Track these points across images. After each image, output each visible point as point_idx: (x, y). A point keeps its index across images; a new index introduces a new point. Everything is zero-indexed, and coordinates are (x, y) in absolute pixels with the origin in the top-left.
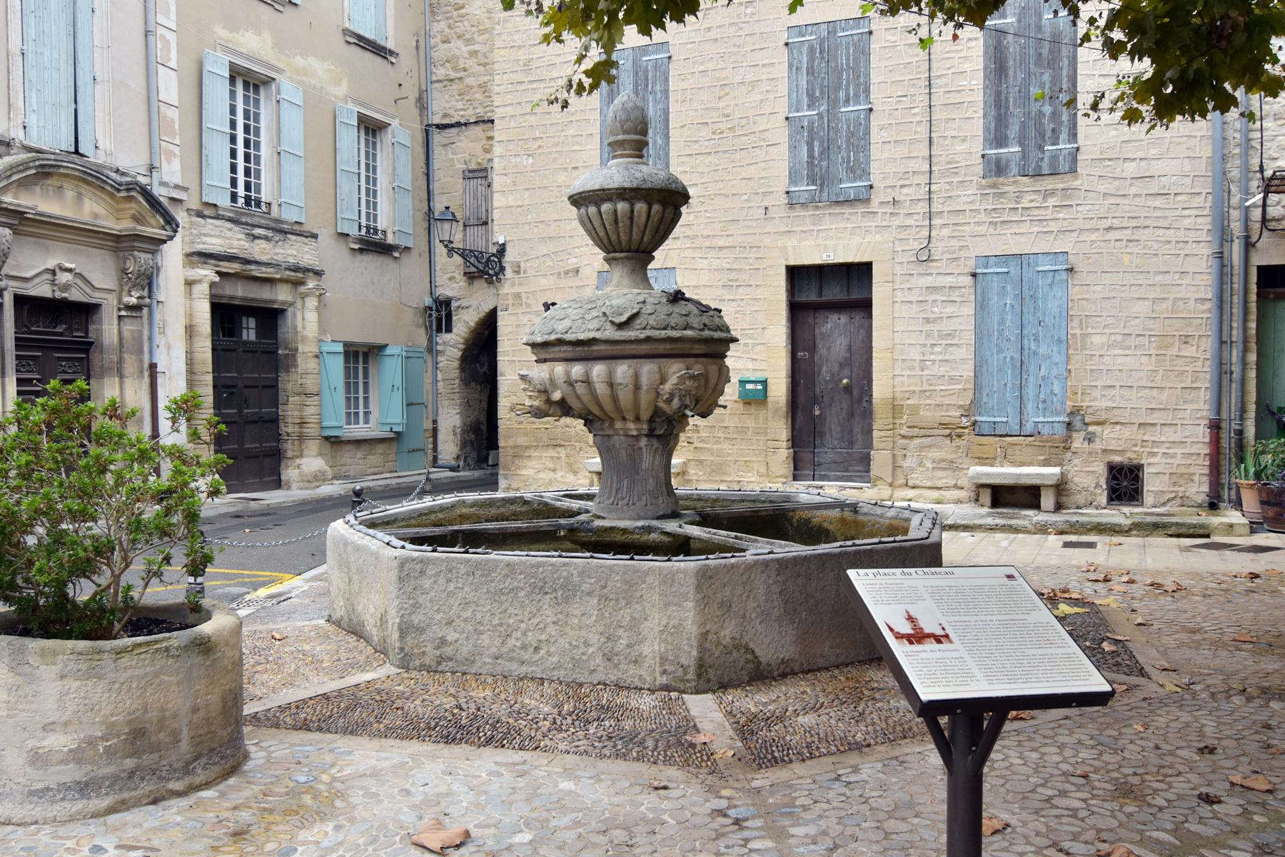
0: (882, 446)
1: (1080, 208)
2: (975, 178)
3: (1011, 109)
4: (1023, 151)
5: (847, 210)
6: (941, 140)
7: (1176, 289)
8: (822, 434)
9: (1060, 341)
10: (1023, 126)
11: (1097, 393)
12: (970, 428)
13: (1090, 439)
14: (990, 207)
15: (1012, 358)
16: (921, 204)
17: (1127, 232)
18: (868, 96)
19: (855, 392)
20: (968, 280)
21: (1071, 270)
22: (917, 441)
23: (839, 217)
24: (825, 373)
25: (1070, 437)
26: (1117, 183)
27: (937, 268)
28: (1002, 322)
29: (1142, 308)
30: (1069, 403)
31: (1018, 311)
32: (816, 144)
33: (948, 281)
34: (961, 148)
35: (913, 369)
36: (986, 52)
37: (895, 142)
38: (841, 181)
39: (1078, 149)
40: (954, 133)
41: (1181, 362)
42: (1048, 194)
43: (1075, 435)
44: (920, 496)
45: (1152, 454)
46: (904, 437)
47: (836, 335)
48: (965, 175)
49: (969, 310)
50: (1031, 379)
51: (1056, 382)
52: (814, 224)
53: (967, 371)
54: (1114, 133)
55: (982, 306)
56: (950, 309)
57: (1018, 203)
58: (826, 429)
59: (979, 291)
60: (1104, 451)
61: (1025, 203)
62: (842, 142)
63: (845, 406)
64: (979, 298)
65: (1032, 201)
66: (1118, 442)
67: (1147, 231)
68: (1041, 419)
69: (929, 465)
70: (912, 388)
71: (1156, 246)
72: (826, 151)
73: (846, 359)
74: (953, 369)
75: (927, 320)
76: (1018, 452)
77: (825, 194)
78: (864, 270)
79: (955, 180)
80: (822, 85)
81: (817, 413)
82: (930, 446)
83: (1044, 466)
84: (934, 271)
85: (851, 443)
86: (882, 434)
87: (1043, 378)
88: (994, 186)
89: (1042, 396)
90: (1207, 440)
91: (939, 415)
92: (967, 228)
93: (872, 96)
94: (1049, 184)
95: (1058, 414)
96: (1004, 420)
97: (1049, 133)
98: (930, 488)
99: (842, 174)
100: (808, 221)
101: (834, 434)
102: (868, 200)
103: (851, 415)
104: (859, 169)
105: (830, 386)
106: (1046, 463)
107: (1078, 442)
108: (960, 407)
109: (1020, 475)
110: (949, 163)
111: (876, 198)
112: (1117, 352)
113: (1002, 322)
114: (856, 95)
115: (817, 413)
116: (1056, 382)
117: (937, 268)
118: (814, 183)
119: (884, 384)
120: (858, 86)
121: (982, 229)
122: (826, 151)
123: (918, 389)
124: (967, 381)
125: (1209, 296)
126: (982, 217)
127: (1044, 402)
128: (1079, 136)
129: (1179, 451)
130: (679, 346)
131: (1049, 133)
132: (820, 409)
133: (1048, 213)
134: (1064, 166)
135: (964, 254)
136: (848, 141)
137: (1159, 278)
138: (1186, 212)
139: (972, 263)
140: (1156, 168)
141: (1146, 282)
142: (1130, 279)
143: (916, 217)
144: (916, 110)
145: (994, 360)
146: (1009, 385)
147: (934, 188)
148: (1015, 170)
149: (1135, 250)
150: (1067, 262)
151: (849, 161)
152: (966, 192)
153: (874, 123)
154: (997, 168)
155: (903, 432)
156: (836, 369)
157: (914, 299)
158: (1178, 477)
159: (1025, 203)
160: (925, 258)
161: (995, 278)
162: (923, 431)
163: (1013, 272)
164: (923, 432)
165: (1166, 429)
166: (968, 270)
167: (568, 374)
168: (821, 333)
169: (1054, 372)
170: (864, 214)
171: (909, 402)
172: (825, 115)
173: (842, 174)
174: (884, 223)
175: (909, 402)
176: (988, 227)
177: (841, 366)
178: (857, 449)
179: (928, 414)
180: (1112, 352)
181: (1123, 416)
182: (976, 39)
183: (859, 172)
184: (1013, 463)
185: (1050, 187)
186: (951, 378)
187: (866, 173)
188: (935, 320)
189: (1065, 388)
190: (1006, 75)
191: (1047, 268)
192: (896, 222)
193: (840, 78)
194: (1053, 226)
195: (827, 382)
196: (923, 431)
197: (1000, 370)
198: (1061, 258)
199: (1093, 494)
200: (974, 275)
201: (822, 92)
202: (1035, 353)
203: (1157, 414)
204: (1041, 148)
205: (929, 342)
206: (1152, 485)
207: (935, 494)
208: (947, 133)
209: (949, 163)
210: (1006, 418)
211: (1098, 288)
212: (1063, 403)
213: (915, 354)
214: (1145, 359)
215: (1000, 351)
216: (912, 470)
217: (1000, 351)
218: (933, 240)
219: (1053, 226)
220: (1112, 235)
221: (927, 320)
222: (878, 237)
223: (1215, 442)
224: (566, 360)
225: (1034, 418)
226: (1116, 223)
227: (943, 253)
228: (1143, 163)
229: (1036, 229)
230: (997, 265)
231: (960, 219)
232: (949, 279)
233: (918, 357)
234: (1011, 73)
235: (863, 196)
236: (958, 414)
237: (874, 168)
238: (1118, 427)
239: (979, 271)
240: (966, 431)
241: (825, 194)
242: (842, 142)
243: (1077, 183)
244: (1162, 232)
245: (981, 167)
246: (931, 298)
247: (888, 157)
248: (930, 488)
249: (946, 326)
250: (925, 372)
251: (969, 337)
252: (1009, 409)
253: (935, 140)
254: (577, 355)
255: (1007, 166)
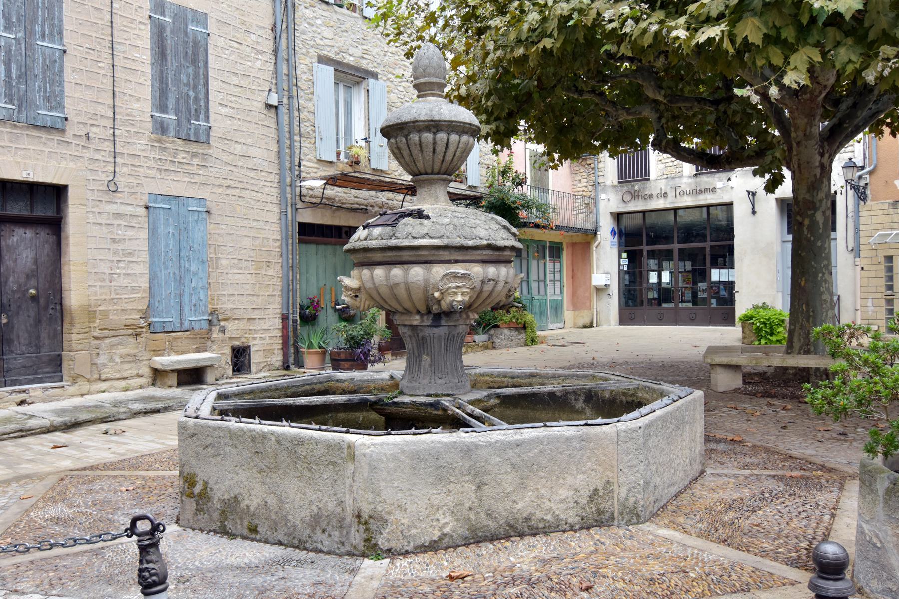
0: (80, 347)
1: (212, 170)
2: (147, 132)
3: (170, 86)
4: (178, 120)
5: (44, 135)
6: (121, 95)
7: (263, 231)
8: (10, 342)
9: (203, 262)
10: (178, 101)
11: (225, 299)
12: (148, 328)
13: (223, 330)
14: (158, 157)
15: (174, 273)
16: (107, 143)
17: (238, 190)
18: (62, 39)
19: (42, 301)
20: (143, 211)
21: (208, 212)
22: (108, 341)
23: (37, 140)
24: (12, 284)
25: (211, 330)
26: (232, 156)
27: (120, 198)
28: (167, 245)
29: (247, 242)
30: (210, 307)
31: (177, 238)
32: (14, 67)
33: (129, 209)
34: (136, 106)
35: (104, 280)
36: (152, 38)
37: (86, 86)
38: (38, 107)
39: (210, 128)
40: (130, 92)
41: (266, 278)
42: (195, 155)
43: (214, 329)
44: (111, 387)
45: (254, 339)
46: (96, 338)
47: (22, 247)
48: (140, 128)
49: (144, 235)
50: (187, 289)
51: (201, 292)
52: (11, 141)
53: (144, 283)
54: (229, 122)
55: (153, 232)
56: (130, 233)
57: (175, 157)
58: (14, 337)
59: (151, 221)
60: (230, 338)
61: (179, 159)
62: (38, 71)
63: (32, 314)
64: (151, 226)
65: (184, 158)
66: (236, 331)
67: (247, 192)
68: (194, 319)
69: (118, 360)
70: (103, 297)
71: (253, 202)
72: (24, 76)
73: (33, 271)
74: (134, 281)
75: (114, 240)
76: (180, 344)
77: (24, 116)
78: (58, 192)
79: (133, 130)
80: (18, 14)
81: (5, 321)
82: (118, 345)
83: (196, 352)
84: (119, 201)
85: (39, 348)
86: (80, 336)
87: (194, 289)
88: (160, 141)
89: (193, 302)
90: (280, 327)
91: (125, 319)
92: (141, 170)
93: (65, 40)
94: (194, 148)
95: (203, 314)
96: (171, 320)
97: (193, 112)
98: (118, 379)
99: (39, 101)
100: (6, 137)
101: (22, 341)
102: (63, 131)
103: (38, 322)
104: (55, 100)
105: (17, 296)
106: (198, 351)
107: (216, 334)
108: (140, 311)
109: (199, 360)
110: (128, 115)
111: (72, 130)
112: (236, 271)
113: (167, 245)
114: (52, 35)
115: (5, 321)
116: (201, 292)
117: (120, 198)
118: (11, 102)
119: (77, 292)
120: (52, 26)
121: (152, 173)
122: (24, 76)
123: (108, 297)
124: (144, 291)
125: (279, 238)
126: (152, 163)
127: (195, 306)
128: (211, 118)
129: (267, 335)
130: (389, 254)
131: (193, 112)
132: (8, 317)
133: (194, 169)
134: (203, 138)
135: (139, 190)
136: (44, 73)
137: (255, 223)
138: (266, 183)
139: (145, 198)
140: (253, 152)
141: (249, 225)
142: (240, 223)
143: (103, 153)
144: (101, 65)
145: (163, 275)
146: (173, 294)
147: (117, 132)
148: (172, 133)
149: (242, 203)
150: (205, 206)
151: (45, 91)
152: (139, 142)
153: (67, 64)
154: (161, 128)
155: (96, 334)
156: (23, 280)
157: (104, 222)
158: (268, 352)
159: (179, 159)
160: (112, 188)
161: (162, 211)
162: (113, 332)
163: (173, 208)
164: (112, 333)
165: (261, 322)
166: (143, 203)
167: (387, 277)
168: (8, 246)
169: (200, 285)
170: (61, 142)
171: (100, 308)
172: (23, 42)
173: (39, 101)
174: (77, 154)
175: (100, 308)
176: (154, 172)
177: (28, 277)
178: (45, 352)
179: (116, 318)
180: (232, 271)
181: (239, 314)
182: (145, 24)
183: (54, 104)
184: (178, 353)
185: (195, 150)
186: (133, 288)
187: (60, 106)
188: (120, 241)
189: (206, 295)
190: (166, 60)
191: (195, 208)
192: (88, 154)
193: (36, 13)
194: (197, 179)
195: (14, 291)
196: (113, 332)
197: (166, 283)
198: (202, 203)
199: (224, 369)
200: (147, 207)
201: (19, 20)
202: (188, 270)
203: (256, 312)
204: (189, 121)
205: (116, 258)
206: (256, 358)
207: (123, 384)
208: (125, 91)
209: (128, 115)
210: (171, 319)
211: (224, 227)
212: (206, 307)
213: (104, 268)
214: (249, 276)
215: (166, 268)
216: (104, 365)
217: (166, 268)
218: (117, 175)
219: (197, 179)
220: (231, 191)
221: (114, 240)
222: (72, 165)
223: (285, 328)
224: (484, 262)
225: (190, 318)
226: (232, 183)
227: (125, 186)
228: (245, 147)
229: (186, 179)
230: (163, 201)
231: (136, 162)
232: (130, 208)
233: (108, 271)
234: (169, 58)
235: (59, 125)
236: (138, 317)
237: (67, 102)
238: (237, 322)
239: (151, 205)
240: (144, 330)
241: (24, 116)
242: (38, 71)
243: (210, 151)
244: (255, 194)
245: (150, 124)
246: (116, 222)
247: (80, 97)
248: (118, 379)
249: (127, 246)
250: (113, 283)
251: (145, 256)
252: (173, 312)
253: (117, 94)
254: (494, 258)
255: (168, 128)
